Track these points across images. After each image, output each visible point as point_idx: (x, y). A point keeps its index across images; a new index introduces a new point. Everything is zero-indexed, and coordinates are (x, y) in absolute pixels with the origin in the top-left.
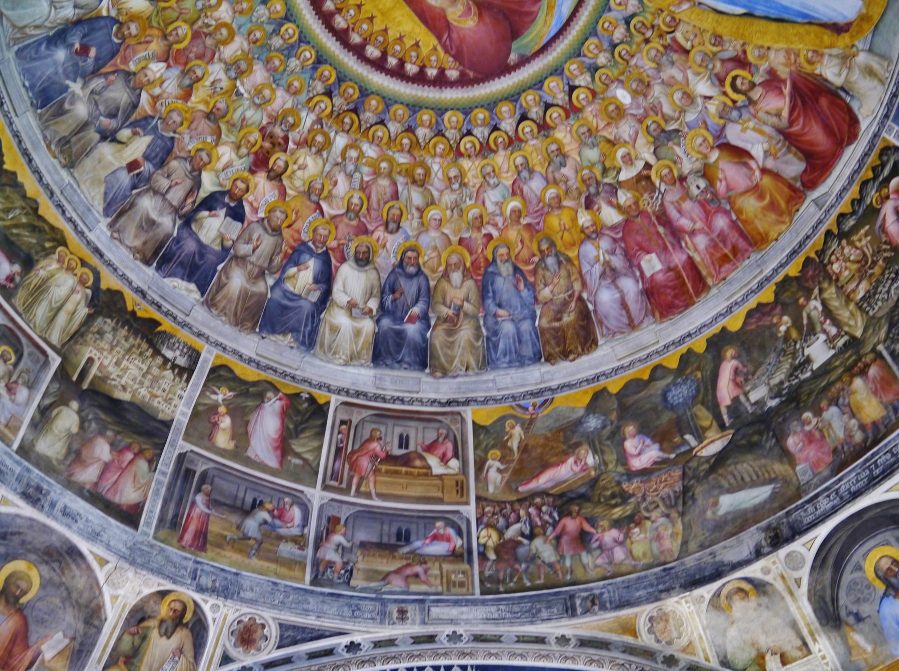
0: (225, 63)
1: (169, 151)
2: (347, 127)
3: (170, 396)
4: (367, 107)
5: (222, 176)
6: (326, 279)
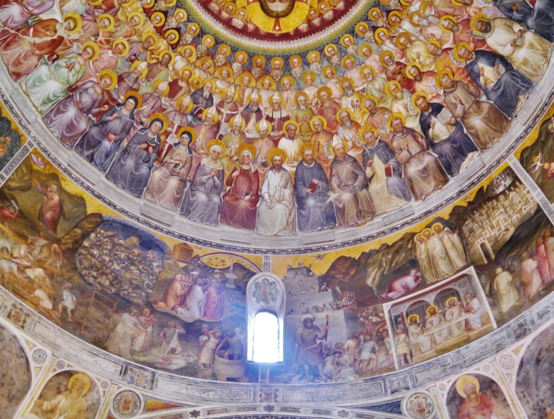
0: (342, 96)
1: (387, 146)
2: (398, 19)
3: (525, 199)
4: (387, 4)
5: (411, 113)
6: (493, 57)
